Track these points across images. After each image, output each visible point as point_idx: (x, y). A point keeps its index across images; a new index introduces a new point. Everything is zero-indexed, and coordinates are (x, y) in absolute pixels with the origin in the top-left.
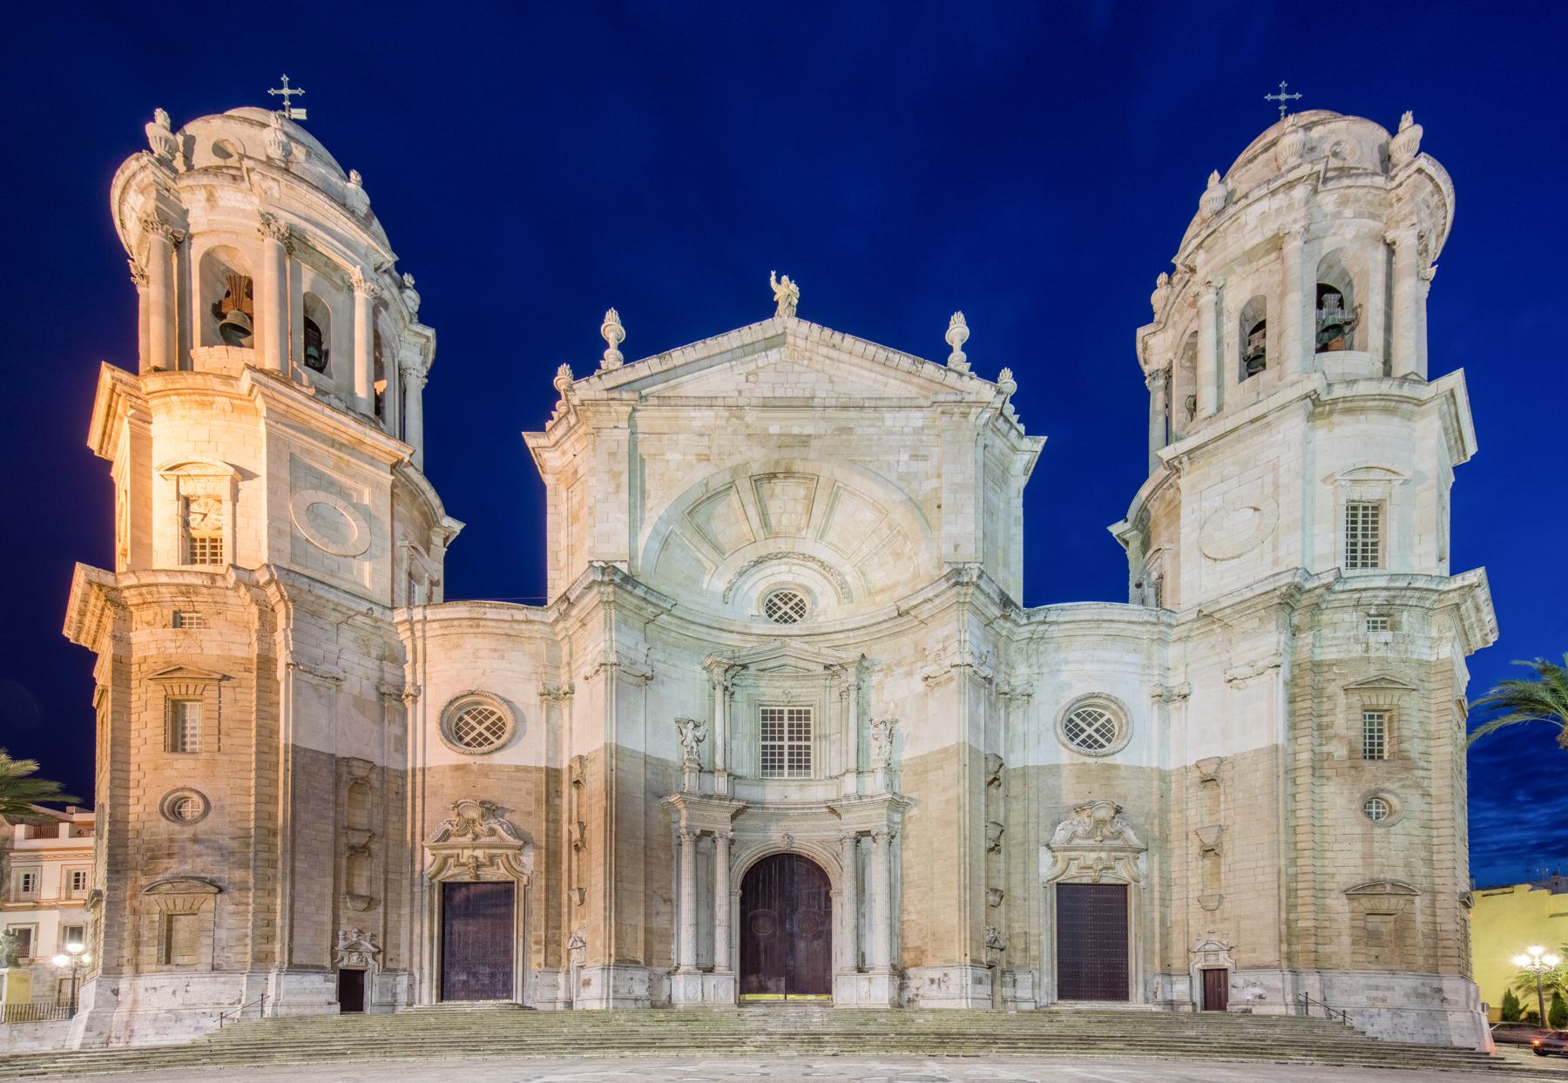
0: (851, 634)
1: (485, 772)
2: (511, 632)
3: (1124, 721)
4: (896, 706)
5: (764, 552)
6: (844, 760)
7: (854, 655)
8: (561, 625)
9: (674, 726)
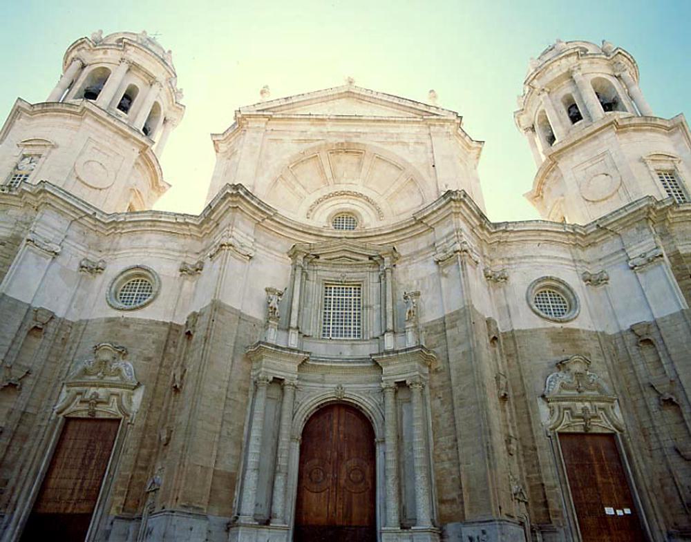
0: (386, 237)
1: (126, 324)
4: (418, 283)
6: (383, 323)
8: (205, 226)
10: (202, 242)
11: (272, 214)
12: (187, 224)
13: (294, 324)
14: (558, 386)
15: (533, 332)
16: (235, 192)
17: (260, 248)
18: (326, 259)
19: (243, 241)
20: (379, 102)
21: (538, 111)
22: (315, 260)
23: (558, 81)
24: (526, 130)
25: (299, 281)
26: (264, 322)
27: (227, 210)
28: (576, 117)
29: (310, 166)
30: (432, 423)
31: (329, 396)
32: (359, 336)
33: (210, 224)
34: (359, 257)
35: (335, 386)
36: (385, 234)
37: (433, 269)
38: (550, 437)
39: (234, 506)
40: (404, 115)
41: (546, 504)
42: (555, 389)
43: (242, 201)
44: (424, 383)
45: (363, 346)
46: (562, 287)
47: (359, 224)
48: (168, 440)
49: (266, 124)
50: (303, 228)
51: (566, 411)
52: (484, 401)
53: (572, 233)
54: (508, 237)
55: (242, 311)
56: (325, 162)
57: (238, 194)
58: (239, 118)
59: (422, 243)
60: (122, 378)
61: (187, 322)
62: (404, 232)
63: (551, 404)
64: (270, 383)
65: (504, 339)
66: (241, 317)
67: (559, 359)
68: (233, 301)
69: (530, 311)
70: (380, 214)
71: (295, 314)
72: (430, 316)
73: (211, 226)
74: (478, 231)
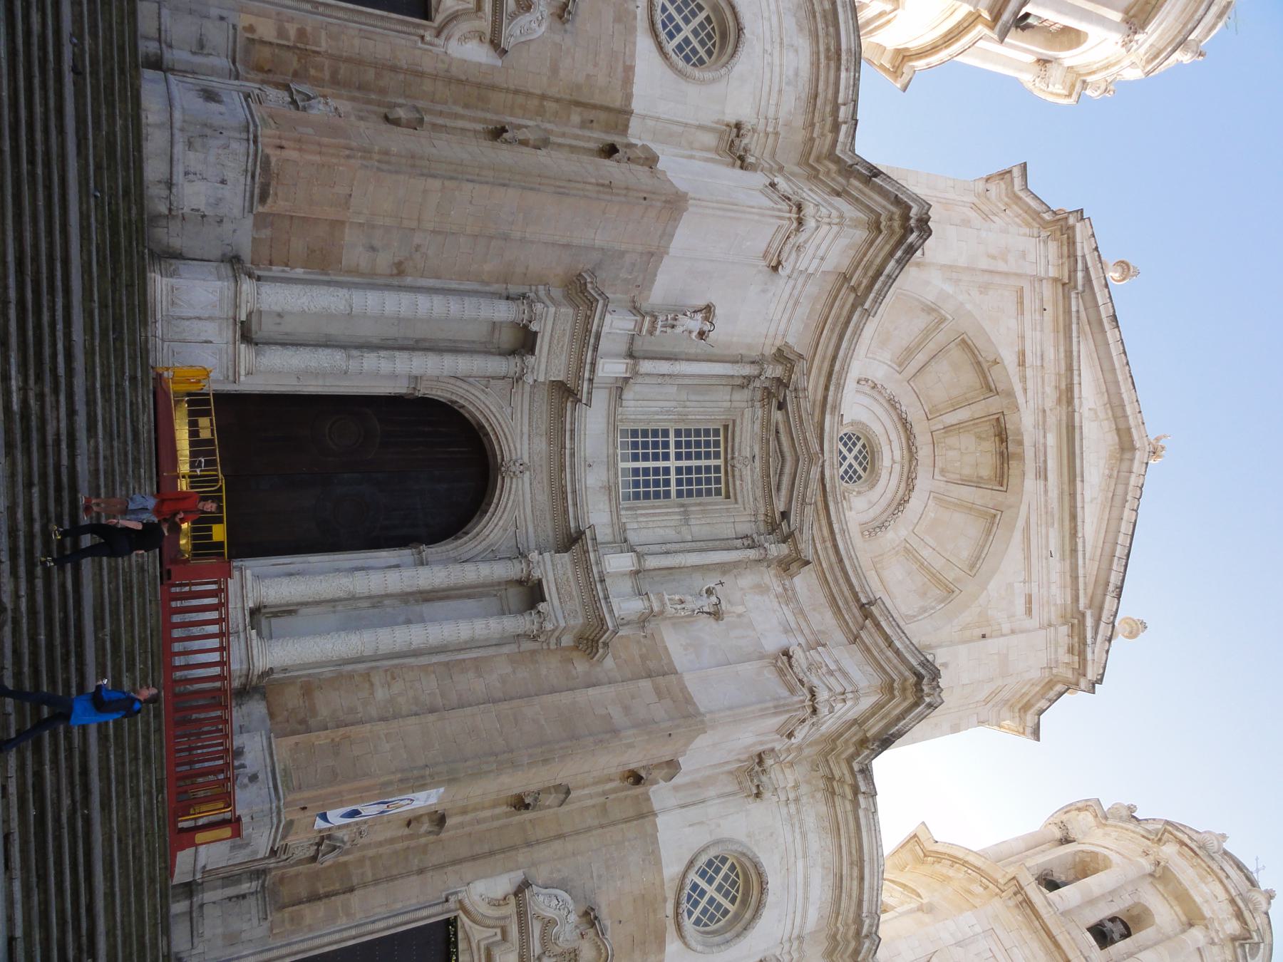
2: (819, 102)
3: (728, 936)
4: (740, 616)
5: (916, 430)
7: (808, 553)
8: (833, 167)
9: (702, 303)
10: (799, 164)
11: (867, 306)
12: (836, 127)
13: (646, 366)
14: (550, 913)
15: (653, 857)
16: (912, 223)
17: (794, 287)
18: (777, 423)
19: (810, 250)
20: (1115, 513)
21: (1106, 852)
22: (774, 403)
23: (1182, 897)
24: (1063, 826)
25: (731, 373)
26: (645, 306)
27: (872, 211)
28: (1102, 935)
29: (969, 378)
30: (464, 660)
31: (505, 448)
32: (626, 497)
33: (840, 179)
34: (784, 492)
35: (526, 459)
36: (834, 540)
37: (773, 643)
38: (447, 900)
39: (274, 268)
40: (1088, 568)
41: (314, 898)
42: (543, 903)
43: (892, 242)
44: (542, 638)
45: (607, 509)
46: (748, 915)
47: (850, 486)
48: (396, 122)
49: (1056, 280)
50: (840, 374)
51: (499, 931)
52: (514, 765)
53: (858, 933)
54: (844, 797)
55: (666, 260)
56: (978, 410)
57: (908, 230)
58: (1066, 218)
59: (825, 620)
60: (513, 16)
61: (635, 145)
62: (841, 581)
63: (512, 900)
64: (526, 327)
65: (637, 797)
66: (653, 257)
67: (604, 913)
68: (685, 237)
69: (696, 847)
70: (876, 528)
71: (664, 367)
72: (674, 642)
73: (833, 179)
74: (854, 735)
